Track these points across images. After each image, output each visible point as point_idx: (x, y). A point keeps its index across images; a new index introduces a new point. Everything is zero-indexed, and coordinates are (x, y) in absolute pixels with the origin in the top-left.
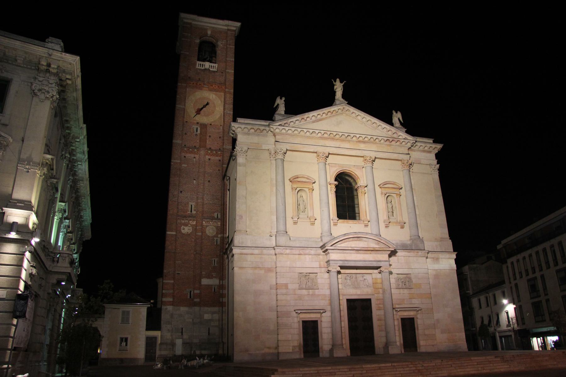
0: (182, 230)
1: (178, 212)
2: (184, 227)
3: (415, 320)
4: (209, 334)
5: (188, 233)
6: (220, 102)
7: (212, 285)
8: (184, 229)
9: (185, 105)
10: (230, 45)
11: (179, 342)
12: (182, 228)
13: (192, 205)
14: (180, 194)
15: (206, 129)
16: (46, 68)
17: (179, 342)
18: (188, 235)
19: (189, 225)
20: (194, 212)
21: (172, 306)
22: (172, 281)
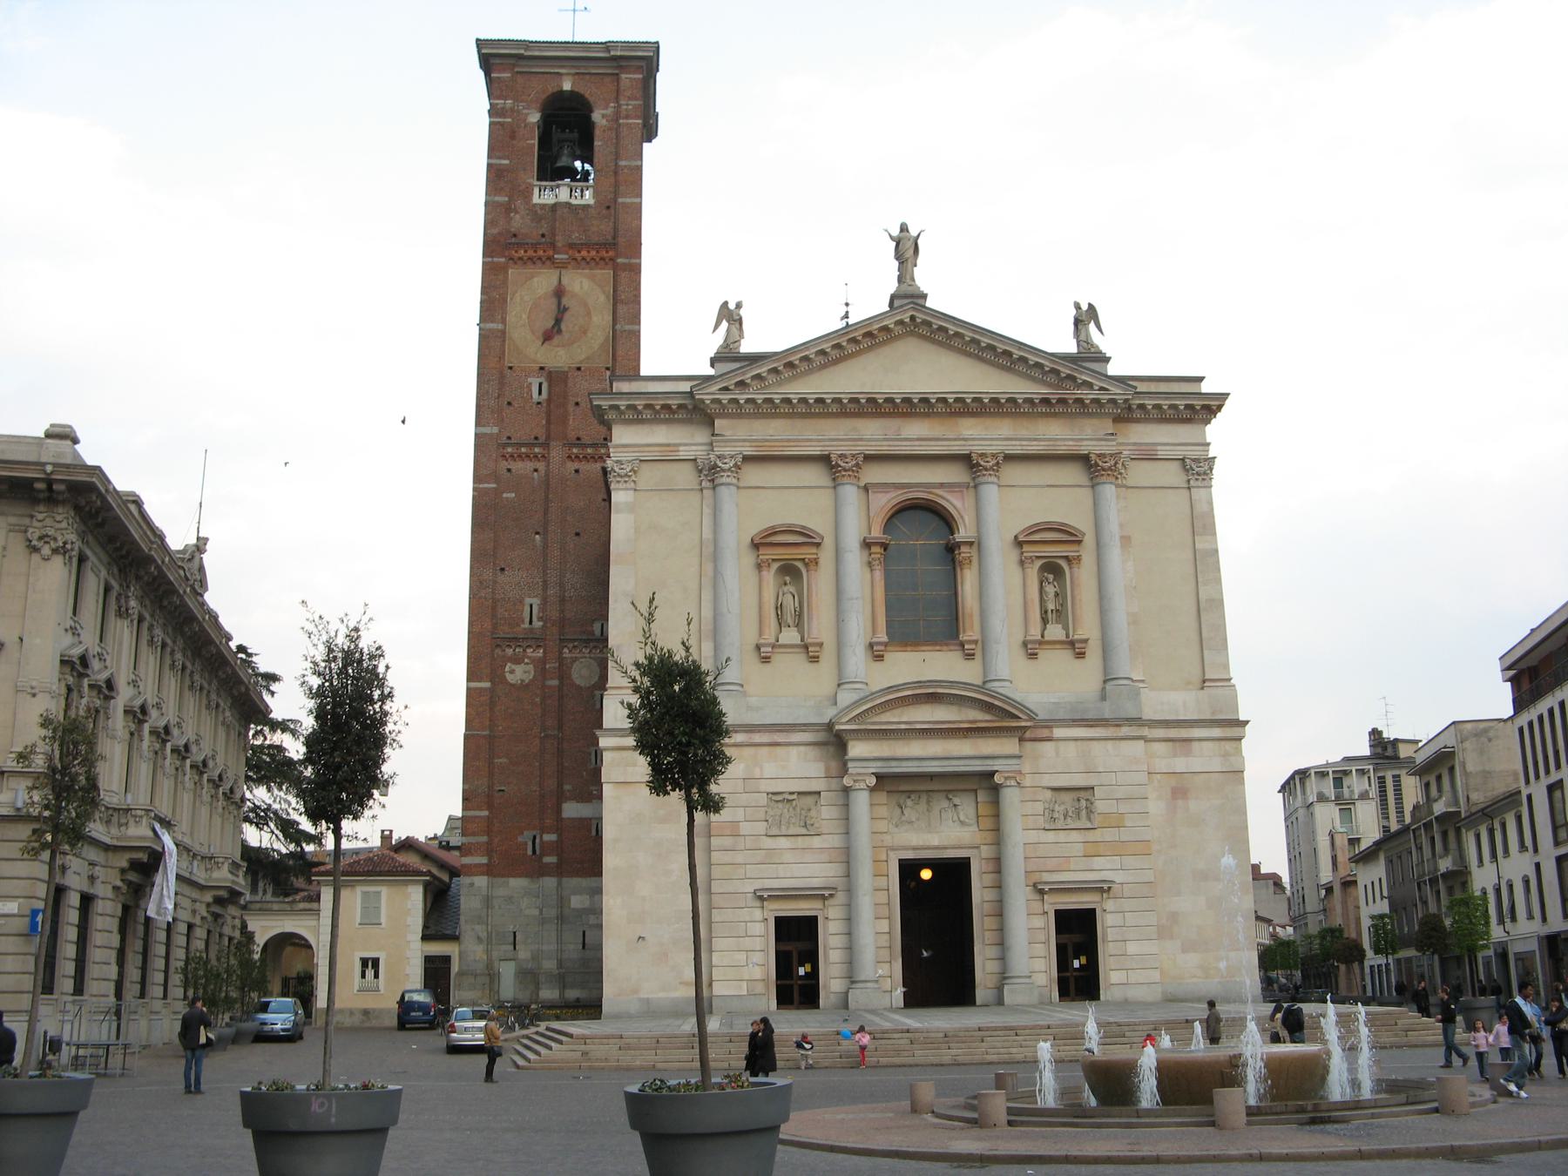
0: (507, 675)
1: (495, 626)
2: (513, 667)
3: (1098, 912)
4: (584, 947)
5: (522, 681)
6: (602, 298)
7: (590, 819)
8: (512, 672)
9: (504, 321)
10: (627, 117)
11: (507, 971)
12: (507, 669)
13: (531, 606)
14: (501, 578)
15: (566, 386)
16: (47, 494)
17: (507, 971)
18: (524, 687)
19: (526, 660)
20: (537, 624)
21: (486, 877)
22: (486, 813)
